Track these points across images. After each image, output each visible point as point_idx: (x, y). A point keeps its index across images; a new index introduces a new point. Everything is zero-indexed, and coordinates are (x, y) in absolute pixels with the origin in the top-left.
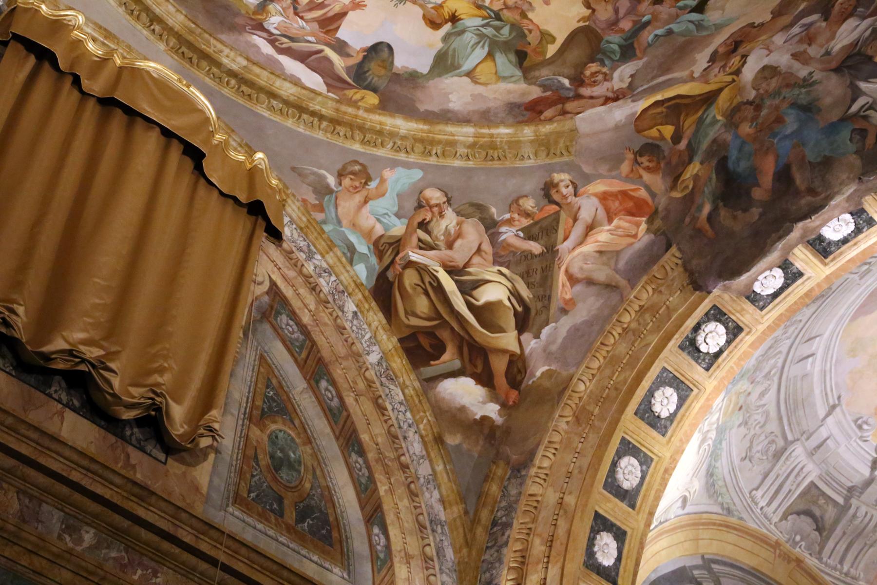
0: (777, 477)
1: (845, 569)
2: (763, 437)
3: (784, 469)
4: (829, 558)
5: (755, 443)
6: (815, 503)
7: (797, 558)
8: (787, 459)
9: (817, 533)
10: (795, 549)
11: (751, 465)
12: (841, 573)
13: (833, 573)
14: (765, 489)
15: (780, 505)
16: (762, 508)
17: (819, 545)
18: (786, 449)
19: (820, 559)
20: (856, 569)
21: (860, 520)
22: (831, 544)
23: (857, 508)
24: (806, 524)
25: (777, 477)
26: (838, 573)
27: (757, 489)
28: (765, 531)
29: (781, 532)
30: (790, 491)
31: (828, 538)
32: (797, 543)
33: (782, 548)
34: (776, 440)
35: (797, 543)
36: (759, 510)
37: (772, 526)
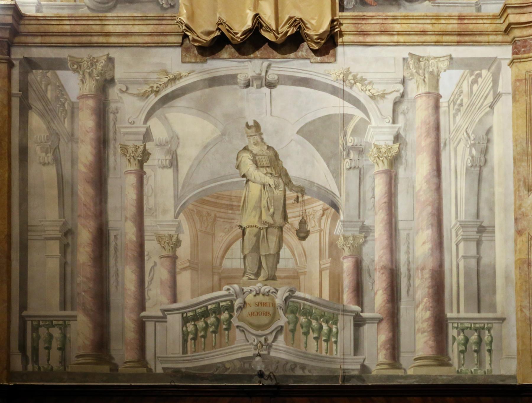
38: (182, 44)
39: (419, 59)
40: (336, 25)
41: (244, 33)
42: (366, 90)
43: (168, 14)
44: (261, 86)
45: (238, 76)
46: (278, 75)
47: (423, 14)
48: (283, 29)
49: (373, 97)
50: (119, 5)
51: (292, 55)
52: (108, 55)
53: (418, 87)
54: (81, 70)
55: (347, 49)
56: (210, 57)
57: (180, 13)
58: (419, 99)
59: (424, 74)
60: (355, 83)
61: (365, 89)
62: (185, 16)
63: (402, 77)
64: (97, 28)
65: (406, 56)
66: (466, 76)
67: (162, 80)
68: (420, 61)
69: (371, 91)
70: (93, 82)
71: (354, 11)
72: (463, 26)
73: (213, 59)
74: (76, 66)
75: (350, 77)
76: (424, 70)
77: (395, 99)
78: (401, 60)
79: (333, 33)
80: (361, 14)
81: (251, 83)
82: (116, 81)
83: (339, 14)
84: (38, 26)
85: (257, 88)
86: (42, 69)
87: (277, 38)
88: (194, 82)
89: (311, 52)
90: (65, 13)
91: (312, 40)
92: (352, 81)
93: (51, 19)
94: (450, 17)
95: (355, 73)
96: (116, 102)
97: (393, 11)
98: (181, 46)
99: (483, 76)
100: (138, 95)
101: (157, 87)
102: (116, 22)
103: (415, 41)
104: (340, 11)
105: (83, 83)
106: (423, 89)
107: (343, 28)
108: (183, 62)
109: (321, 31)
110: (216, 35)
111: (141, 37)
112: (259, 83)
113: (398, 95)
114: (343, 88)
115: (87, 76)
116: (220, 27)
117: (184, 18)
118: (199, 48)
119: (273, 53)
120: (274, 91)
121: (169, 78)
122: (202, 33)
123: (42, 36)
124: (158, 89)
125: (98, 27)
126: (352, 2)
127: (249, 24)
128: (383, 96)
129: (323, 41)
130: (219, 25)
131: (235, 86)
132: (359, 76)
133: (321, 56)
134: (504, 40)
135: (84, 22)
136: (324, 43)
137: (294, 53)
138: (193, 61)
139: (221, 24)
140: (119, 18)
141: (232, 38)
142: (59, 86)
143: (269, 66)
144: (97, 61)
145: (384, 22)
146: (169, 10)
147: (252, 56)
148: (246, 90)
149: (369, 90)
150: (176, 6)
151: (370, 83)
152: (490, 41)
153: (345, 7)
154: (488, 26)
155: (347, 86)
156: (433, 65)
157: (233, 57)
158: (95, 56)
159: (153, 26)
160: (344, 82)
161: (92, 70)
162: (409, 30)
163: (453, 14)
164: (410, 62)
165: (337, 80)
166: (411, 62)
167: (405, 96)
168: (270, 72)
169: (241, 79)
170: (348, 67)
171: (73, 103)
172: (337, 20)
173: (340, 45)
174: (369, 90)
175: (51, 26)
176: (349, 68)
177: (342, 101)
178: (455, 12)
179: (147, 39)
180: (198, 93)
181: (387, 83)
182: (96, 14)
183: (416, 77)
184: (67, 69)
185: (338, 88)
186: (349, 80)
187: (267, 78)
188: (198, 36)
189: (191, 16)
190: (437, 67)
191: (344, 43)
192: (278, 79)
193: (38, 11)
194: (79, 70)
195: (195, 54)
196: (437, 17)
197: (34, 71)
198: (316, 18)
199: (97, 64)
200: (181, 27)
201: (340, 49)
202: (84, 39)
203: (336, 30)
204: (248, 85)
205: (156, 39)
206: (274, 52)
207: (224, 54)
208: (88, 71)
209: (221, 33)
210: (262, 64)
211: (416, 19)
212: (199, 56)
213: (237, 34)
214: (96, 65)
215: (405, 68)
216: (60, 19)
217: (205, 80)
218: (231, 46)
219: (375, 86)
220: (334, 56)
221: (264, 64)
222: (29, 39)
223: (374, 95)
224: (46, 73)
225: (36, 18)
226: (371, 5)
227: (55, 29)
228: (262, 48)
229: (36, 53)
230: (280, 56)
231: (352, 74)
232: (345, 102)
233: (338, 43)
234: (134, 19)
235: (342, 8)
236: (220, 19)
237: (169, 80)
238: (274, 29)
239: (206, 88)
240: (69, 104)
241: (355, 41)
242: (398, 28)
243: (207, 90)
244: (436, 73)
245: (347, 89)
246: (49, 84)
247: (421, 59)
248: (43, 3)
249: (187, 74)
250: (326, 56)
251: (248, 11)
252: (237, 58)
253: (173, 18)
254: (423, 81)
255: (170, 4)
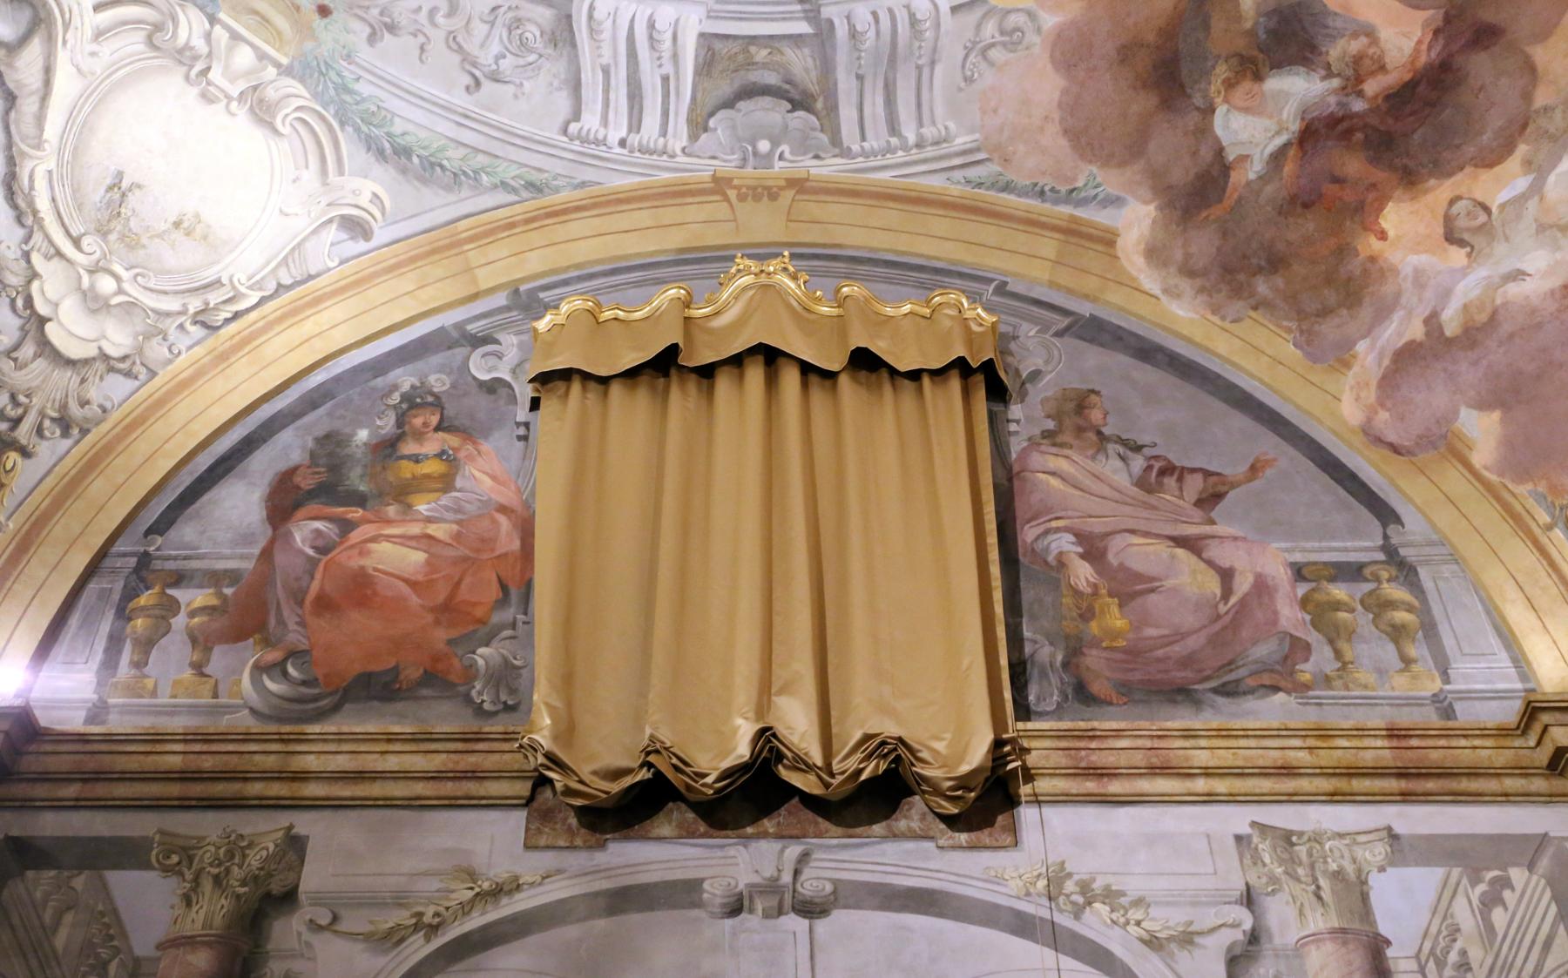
0: (606, 71)
1: (911, 138)
2: (480, 29)
3: (606, 51)
4: (863, 139)
5: (472, 47)
6: (750, 64)
7: (787, 180)
8: (593, 31)
9: (801, 113)
10: (772, 167)
11: (510, 89)
12: (905, 148)
13: (890, 159)
14: (599, 106)
15: (665, 114)
16: (623, 143)
17: (822, 131)
18: (569, 17)
19: (846, 153)
20: (934, 123)
21: (871, 34)
22: (847, 114)
23: (848, 17)
24: (768, 112)
25: (606, 71)
26: (900, 153)
27: (576, 116)
28: (666, 175)
29: (714, 158)
30: (665, 79)
31: (833, 108)
32: (770, 155)
33: (736, 182)
34: (521, 13)
35: (770, 155)
36: (618, 150)
37: (682, 159)
38: (530, 800)
39: (1287, 838)
40: (1009, 754)
41: (727, 774)
42: (1127, 923)
43: (495, 727)
44: (780, 912)
45: (706, 886)
46: (835, 882)
47: (1275, 725)
48: (845, 764)
49: (1152, 943)
50: (347, 706)
51: (877, 828)
52: (291, 827)
53: (1301, 913)
54: (189, 869)
55: (1048, 811)
56: (617, 835)
57: (532, 723)
58: (1313, 947)
59: (1315, 880)
60: (1090, 904)
61: (1122, 920)
62: (546, 732)
63: (1244, 888)
64: (271, 762)
65: (1245, 829)
66: (1458, 884)
67: (453, 896)
68: (1293, 845)
69: (1144, 924)
70: (223, 901)
71: (1060, 719)
72: (1409, 752)
73: (627, 838)
74: (175, 859)
75: (1069, 886)
76: (1312, 866)
77: (1230, 949)
78: (1231, 842)
79: (1001, 772)
80: (1082, 725)
81: (746, 903)
82: (302, 897)
83: (1014, 728)
84: (78, 757)
85: (767, 915)
86: (58, 866)
87: (827, 785)
88: (562, 902)
89: (938, 820)
90: (178, 724)
91: (938, 792)
92: (1080, 900)
93: (128, 739)
94: (1361, 732)
95: (1085, 877)
96: (292, 955)
97: (1180, 719)
98: (526, 805)
99: (1519, 887)
100: (368, 937)
101: (437, 914)
102: (332, 747)
103: (1265, 791)
104: (1017, 719)
105: (189, 904)
106: (1318, 921)
107: (1032, 760)
108: (527, 847)
109: (965, 768)
110: (638, 778)
111: (401, 784)
112: (774, 902)
113: (1238, 935)
114: (1049, 917)
115: (207, 885)
116: (651, 758)
117: (544, 737)
118: (581, 812)
119: (817, 823)
120: (822, 926)
121: (477, 890)
122: (595, 773)
123: (85, 781)
124: (437, 920)
125: (272, 758)
126: (1052, 695)
127: (742, 751)
128: (1187, 939)
129: (973, 794)
130: (648, 753)
131: (695, 913)
132: (1098, 885)
133: (969, 829)
134: (1554, 790)
135: (231, 747)
136: (977, 799)
137: (884, 824)
138: (562, 843)
139: (657, 752)
140: (340, 738)
141: (688, 787)
142: (102, 914)
143: (804, 858)
144: (250, 845)
145: (1157, 744)
146: (501, 716)
147: (749, 830)
148: (729, 922)
149: (1138, 923)
150: (523, 707)
151: (1139, 902)
152: (1510, 791)
153: (1033, 707)
154: (1487, 754)
155: (1061, 911)
156: (1337, 854)
157: (692, 834)
158: (246, 831)
159: (444, 756)
160: (1050, 899)
161: (228, 871)
162: (1240, 763)
163: (1370, 725)
164: (1260, 846)
165: (1028, 894)
166: (1264, 847)
167: (1263, 940)
168: (807, 873)
169: (714, 891)
170: (1059, 860)
171: (137, 961)
172: (1012, 741)
173: (1026, 802)
174: (1138, 923)
175: (124, 758)
176: (1063, 863)
177: (1049, 953)
178: (1376, 718)
179: (420, 788)
180: (571, 932)
181: (1194, 904)
182: (273, 728)
183: (1289, 886)
184: (147, 866)
185: (1034, 917)
186: (1068, 896)
187: (799, 888)
188: (581, 782)
189: (567, 730)
190: (1354, 861)
191: (1040, 798)
192: (834, 892)
193: (90, 720)
194: (185, 870)
195: (570, 829)
196: (1323, 733)
197: (30, 874)
198: (948, 736)
199: (247, 852)
200: (531, 759)
201: (1027, 815)
202: (220, 789)
203: (1010, 766)
204: (735, 908)
205: (449, 788)
206: (820, 820)
207: (663, 826)
208: (215, 871)
209: (654, 774)
210: (782, 851)
211: (1255, 736)
212: (583, 831)
213: (704, 776)
214: (244, 856)
215: (1248, 861)
216: (156, 738)
217: (596, 894)
218: (684, 807)
219: (1153, 911)
220: (1013, 829)
221: (788, 851)
222: (41, 791)
223: (1156, 937)
224: (69, 878)
225: (82, 738)
226: (1110, 703)
227: (132, 764)
228: (783, 811)
229: (49, 825)
230: (840, 830)
231: (1076, 877)
232: (1060, 955)
233: (1019, 796)
234: (391, 738)
235: (1024, 711)
236: (652, 739)
237: (478, 894)
238: (819, 763)
239: (600, 917)
240: (122, 964)
241: (1074, 791)
242: (1202, 758)
243: (601, 924)
244: (1352, 876)
245: (1066, 921)
246: (69, 908)
247: (1294, 839)
248: (112, 701)
249: (539, 879)
250: (986, 831)
251: (740, 721)
252: (702, 836)
253: (508, 737)
254: (1314, 899)
255: (505, 703)
